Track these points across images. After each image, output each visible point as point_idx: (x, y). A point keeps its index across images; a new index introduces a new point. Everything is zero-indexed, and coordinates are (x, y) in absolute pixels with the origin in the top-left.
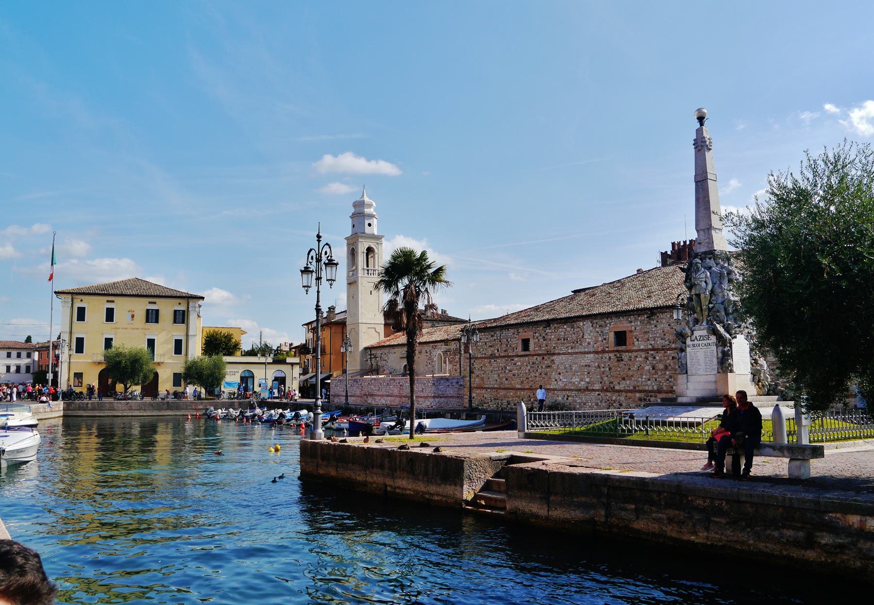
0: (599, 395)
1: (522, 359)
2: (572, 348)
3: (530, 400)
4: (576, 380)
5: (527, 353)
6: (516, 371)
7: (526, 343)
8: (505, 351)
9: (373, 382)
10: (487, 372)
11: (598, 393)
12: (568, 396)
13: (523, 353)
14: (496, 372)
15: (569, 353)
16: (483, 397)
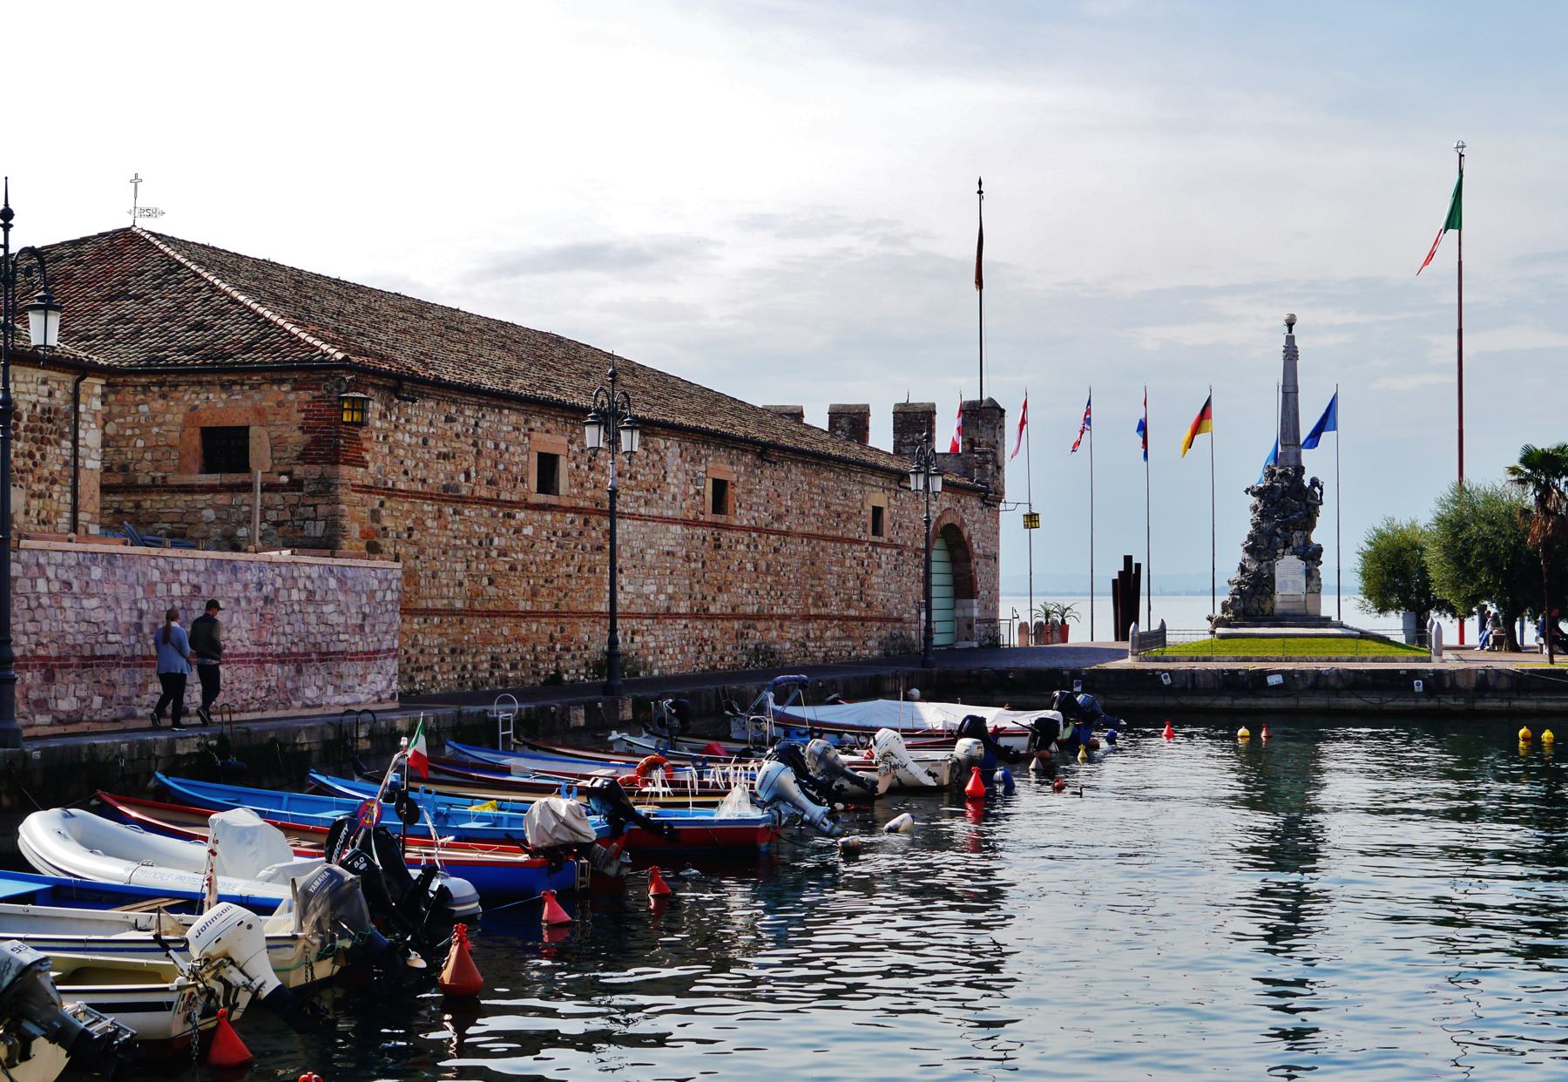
0: (686, 626)
1: (536, 516)
2: (646, 504)
3: (553, 649)
4: (650, 588)
5: (552, 499)
6: (521, 556)
7: (548, 464)
8: (491, 482)
9: (97, 573)
10: (429, 551)
11: (684, 622)
12: (634, 633)
13: (542, 498)
14: (460, 554)
15: (641, 517)
16: (413, 646)
